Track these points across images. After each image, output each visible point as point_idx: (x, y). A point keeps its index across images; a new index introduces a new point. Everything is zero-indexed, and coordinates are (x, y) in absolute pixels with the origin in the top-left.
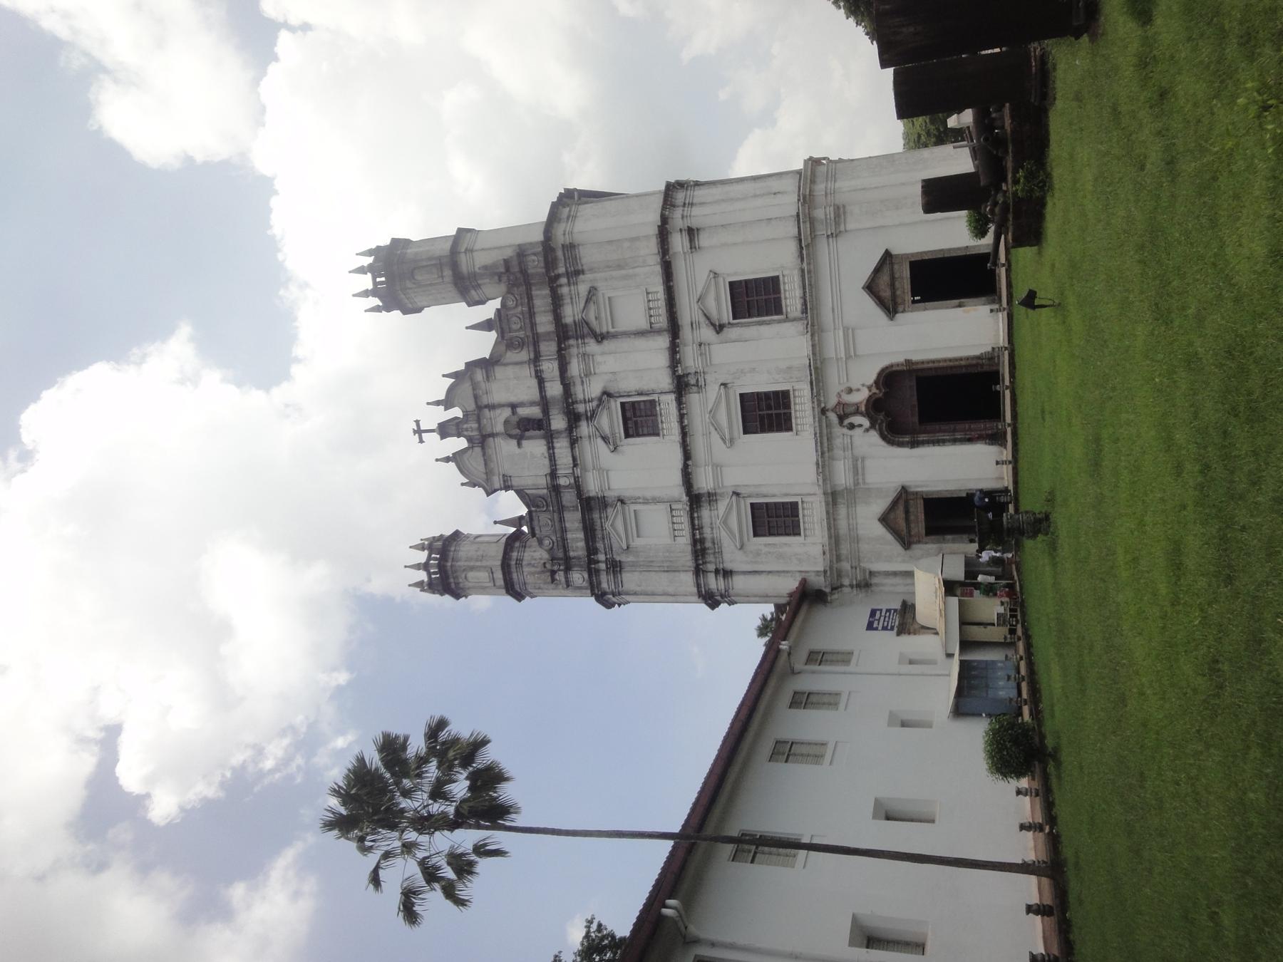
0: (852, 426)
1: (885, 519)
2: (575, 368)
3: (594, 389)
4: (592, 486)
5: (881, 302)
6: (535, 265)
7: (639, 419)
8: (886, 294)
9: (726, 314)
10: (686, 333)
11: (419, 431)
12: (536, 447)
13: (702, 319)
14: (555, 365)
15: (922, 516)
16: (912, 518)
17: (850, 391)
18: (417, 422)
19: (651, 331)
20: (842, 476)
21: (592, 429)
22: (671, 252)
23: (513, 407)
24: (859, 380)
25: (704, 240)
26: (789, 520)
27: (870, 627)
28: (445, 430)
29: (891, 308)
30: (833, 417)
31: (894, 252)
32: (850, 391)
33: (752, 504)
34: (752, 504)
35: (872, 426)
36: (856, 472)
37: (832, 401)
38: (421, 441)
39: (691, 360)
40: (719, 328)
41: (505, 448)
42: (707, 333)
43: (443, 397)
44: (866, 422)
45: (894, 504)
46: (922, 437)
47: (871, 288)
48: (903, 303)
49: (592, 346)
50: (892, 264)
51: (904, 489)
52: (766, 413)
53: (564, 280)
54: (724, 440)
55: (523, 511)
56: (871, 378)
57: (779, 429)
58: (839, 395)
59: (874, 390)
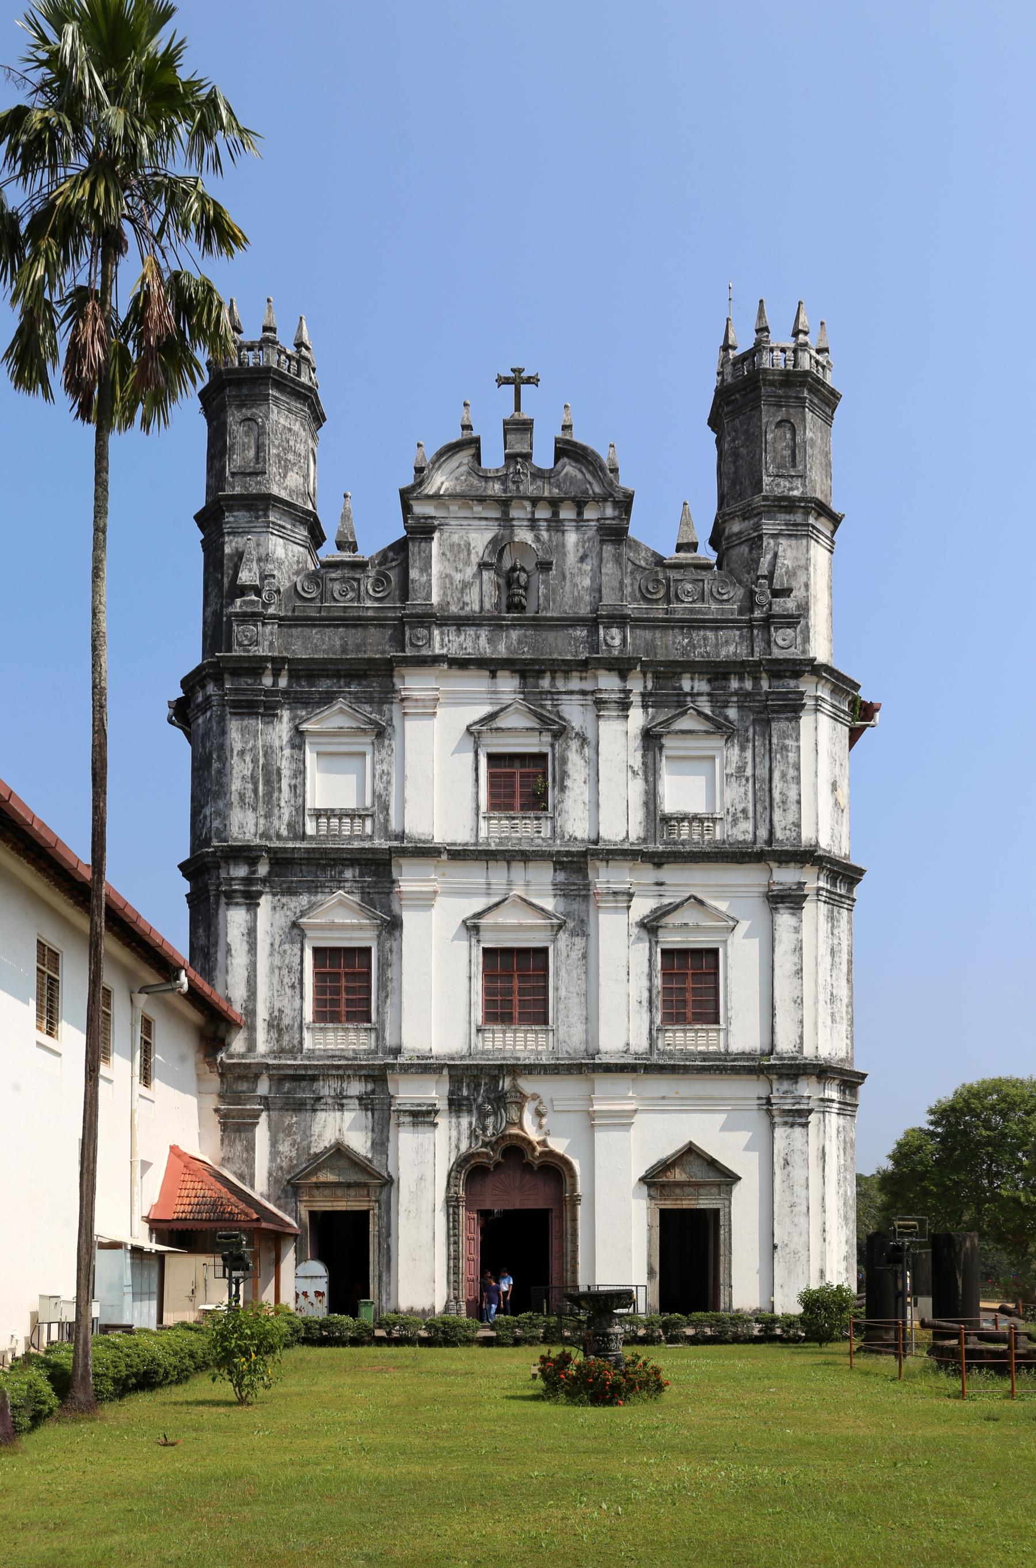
1: (339, 1152)
3: (575, 713)
5: (665, 1166)
8: (678, 1175)
9: (672, 939)
10: (647, 874)
11: (517, 380)
12: (482, 596)
13: (666, 901)
15: (341, 1206)
16: (339, 1192)
17: (539, 1114)
19: (657, 819)
21: (507, 699)
22: (774, 865)
25: (785, 919)
26: (343, 1008)
28: (519, 427)
29: (655, 1180)
31: (737, 1190)
33: (368, 950)
34: (368, 950)
36: (414, 1114)
38: (503, 381)
40: (651, 926)
43: (578, 437)
47: (691, 1151)
48: (663, 1197)
49: (637, 718)
50: (719, 1185)
53: (748, 685)
54: (479, 915)
55: (369, 549)
56: (558, 1145)
57: (488, 1004)
58: (535, 1097)
59: (539, 1149)
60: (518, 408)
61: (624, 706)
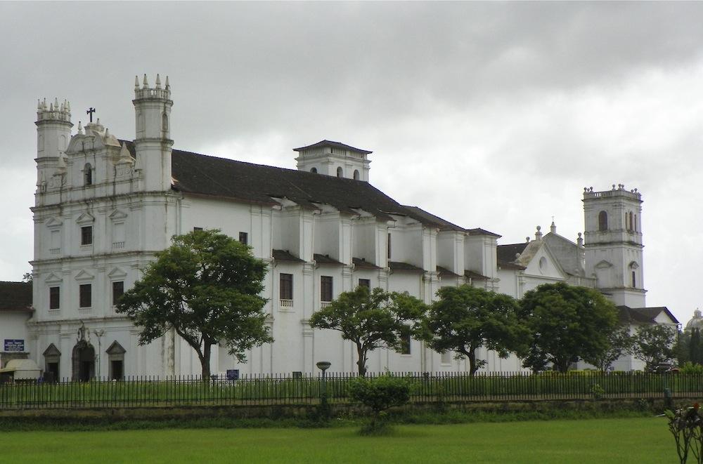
0: (79, 333)
1: (52, 346)
2: (102, 205)
3: (96, 214)
4: (67, 211)
6: (139, 186)
7: (87, 235)
12: (81, 180)
14: (103, 195)
17: (89, 333)
18: (94, 111)
20: (64, 329)
23: (94, 169)
24: (92, 340)
27: (6, 341)
29: (109, 351)
30: (81, 326)
32: (89, 333)
35: (78, 342)
37: (86, 326)
38: (88, 112)
39: (101, 263)
41: (80, 163)
42: (109, 270)
44: (79, 340)
45: (56, 350)
46: (77, 363)
51: (60, 354)
52: (86, 296)
58: (87, 329)
60: (91, 121)
61: (105, 211)
